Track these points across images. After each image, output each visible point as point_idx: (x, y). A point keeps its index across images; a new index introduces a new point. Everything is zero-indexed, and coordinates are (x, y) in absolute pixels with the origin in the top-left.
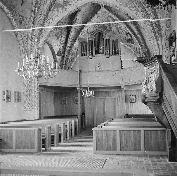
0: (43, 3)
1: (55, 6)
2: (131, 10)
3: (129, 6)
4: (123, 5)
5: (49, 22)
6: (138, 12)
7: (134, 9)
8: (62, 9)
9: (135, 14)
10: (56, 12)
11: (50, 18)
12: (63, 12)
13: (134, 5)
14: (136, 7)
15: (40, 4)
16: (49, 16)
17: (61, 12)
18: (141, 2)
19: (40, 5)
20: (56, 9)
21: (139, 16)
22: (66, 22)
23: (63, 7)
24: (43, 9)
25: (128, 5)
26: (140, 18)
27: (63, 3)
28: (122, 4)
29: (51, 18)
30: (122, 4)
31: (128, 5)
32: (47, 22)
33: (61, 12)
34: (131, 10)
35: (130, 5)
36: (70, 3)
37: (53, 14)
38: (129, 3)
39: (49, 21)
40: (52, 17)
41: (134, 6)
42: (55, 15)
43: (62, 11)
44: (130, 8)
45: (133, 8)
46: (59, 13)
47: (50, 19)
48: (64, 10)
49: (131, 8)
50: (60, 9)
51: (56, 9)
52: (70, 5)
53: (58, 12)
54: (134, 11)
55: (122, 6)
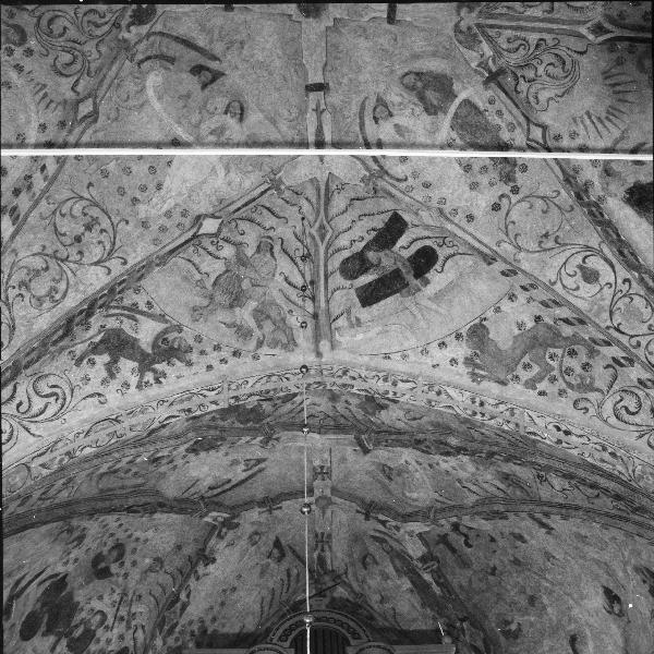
0: (43, 292)
1: (101, 341)
2: (542, 393)
3: (525, 375)
4: (490, 379)
5: (35, 409)
6: (593, 396)
7: (564, 386)
8: (142, 372)
9: (571, 411)
10: (98, 371)
11: (49, 391)
12: (139, 387)
13: (554, 364)
14: (569, 371)
15: (23, 284)
16: (52, 380)
17: (127, 385)
18: (603, 325)
19: (23, 292)
20: (106, 358)
21: (599, 416)
22: (122, 619)
23: (145, 363)
24: (30, 323)
25: (520, 371)
26: (613, 420)
27: (154, 345)
28: (482, 372)
29: (55, 390)
30: (482, 372)
31: (520, 371)
32: (22, 409)
33: (127, 385)
34: (542, 393)
35: (536, 369)
36: (194, 357)
37: (75, 374)
38: (526, 359)
39: (38, 403)
40: (67, 391)
41: (555, 373)
42: (89, 389)
43: (134, 380)
44: (531, 384)
45: (553, 380)
46: (115, 385)
47: (47, 396)
48: (149, 377)
49: (541, 386)
50: (127, 366)
51: (106, 358)
52: (189, 364)
53: (112, 375)
54: (561, 393)
55: (485, 384)
